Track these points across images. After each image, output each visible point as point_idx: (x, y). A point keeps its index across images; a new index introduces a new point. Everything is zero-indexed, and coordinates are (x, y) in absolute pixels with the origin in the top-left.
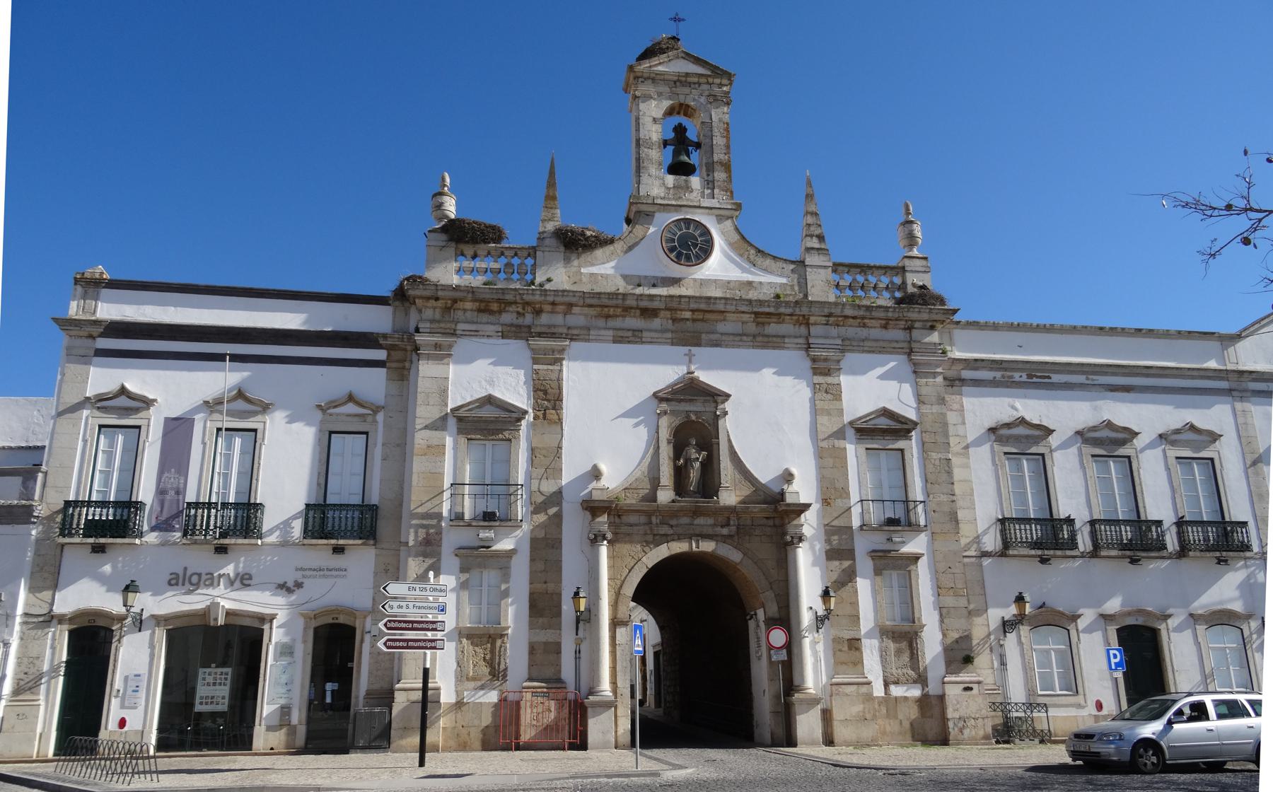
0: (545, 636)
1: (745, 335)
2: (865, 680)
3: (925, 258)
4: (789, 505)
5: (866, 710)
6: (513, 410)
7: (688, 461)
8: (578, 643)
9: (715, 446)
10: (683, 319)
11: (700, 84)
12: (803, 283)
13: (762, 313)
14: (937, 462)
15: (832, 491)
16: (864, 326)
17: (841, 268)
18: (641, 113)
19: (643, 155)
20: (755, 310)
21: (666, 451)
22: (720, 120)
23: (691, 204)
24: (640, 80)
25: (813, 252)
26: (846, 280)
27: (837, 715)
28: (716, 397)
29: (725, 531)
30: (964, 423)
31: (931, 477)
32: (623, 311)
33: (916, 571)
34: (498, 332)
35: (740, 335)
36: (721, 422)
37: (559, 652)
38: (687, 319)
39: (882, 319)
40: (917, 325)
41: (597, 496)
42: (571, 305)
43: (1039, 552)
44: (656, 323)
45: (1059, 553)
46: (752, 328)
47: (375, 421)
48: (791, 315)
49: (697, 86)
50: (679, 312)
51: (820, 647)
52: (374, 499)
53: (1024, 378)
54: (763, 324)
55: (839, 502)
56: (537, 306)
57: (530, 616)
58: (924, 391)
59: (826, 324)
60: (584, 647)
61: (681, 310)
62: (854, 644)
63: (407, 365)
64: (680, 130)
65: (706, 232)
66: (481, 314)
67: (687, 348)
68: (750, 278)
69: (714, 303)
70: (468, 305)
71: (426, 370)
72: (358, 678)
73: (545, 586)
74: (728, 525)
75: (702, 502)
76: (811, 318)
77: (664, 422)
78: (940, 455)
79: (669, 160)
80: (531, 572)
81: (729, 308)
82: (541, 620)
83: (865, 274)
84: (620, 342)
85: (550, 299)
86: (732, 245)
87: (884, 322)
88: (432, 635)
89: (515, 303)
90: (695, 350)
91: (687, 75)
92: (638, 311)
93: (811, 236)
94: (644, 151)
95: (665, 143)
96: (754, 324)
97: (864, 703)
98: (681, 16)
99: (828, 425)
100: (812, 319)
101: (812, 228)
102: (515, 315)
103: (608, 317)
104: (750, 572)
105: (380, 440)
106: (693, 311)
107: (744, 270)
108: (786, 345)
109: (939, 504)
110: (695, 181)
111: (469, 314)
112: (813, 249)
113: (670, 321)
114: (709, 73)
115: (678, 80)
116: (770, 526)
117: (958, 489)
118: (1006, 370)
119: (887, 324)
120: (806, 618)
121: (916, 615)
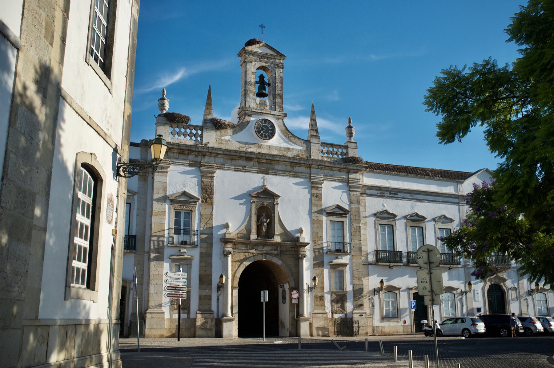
0: (206, 292)
1: (286, 171)
2: (325, 312)
3: (356, 143)
4: (301, 243)
5: (325, 323)
6: (194, 198)
7: (262, 223)
8: (218, 296)
9: (273, 217)
10: (262, 163)
11: (271, 59)
12: (309, 149)
13: (294, 162)
14: (356, 227)
15: (316, 236)
16: (332, 170)
17: (324, 145)
18: (247, 69)
19: (248, 88)
20: (291, 161)
21: (254, 218)
22: (279, 75)
23: (267, 113)
24: (247, 54)
25: (314, 137)
26: (326, 149)
27: (315, 325)
28: (273, 196)
29: (276, 252)
30: (365, 211)
31: (353, 233)
32: (239, 158)
33: (346, 270)
34: (187, 163)
35: (285, 171)
36: (276, 206)
37: (210, 299)
38: (264, 163)
39: (338, 168)
40: (351, 171)
41: (227, 236)
42: (218, 154)
43: (388, 264)
44: (252, 163)
45: (396, 264)
46: (289, 168)
47: (133, 199)
48: (305, 164)
49: (270, 59)
50: (261, 160)
51: (309, 299)
52: (134, 233)
53: (388, 195)
54: (293, 166)
55: (319, 242)
56: (204, 153)
57: (200, 284)
58: (353, 198)
59: (318, 168)
60: (221, 298)
61: (262, 159)
62: (322, 298)
63: (147, 174)
64: (262, 77)
65: (273, 126)
66: (180, 155)
67: (262, 175)
68: (289, 146)
69: (276, 157)
70: (175, 151)
71: (158, 177)
72: (128, 308)
73: (205, 272)
74: (277, 250)
75: (268, 241)
76: (312, 166)
77: (254, 206)
78: (357, 225)
79: (257, 91)
80: (200, 267)
81: (281, 159)
82: (204, 286)
83: (333, 148)
84: (237, 171)
85: (210, 151)
86: (282, 131)
87: (339, 169)
88: (182, 292)
89: (195, 151)
90: (266, 176)
91: (267, 54)
92: (245, 158)
93: (313, 130)
94: (248, 86)
95: (256, 82)
96: (290, 166)
97: (324, 321)
98: (263, 25)
99: (315, 209)
100: (313, 166)
101: (314, 127)
102: (194, 156)
103: (232, 159)
104: (284, 269)
105: (136, 207)
106: (267, 159)
107: (285, 141)
108: (302, 176)
109: (356, 244)
110: (267, 100)
111: (175, 154)
112: (314, 135)
113: (257, 163)
114: (276, 54)
115: (263, 56)
116: (293, 251)
117: (362, 238)
118: (382, 190)
119: (340, 170)
120: (305, 287)
121: (345, 287)
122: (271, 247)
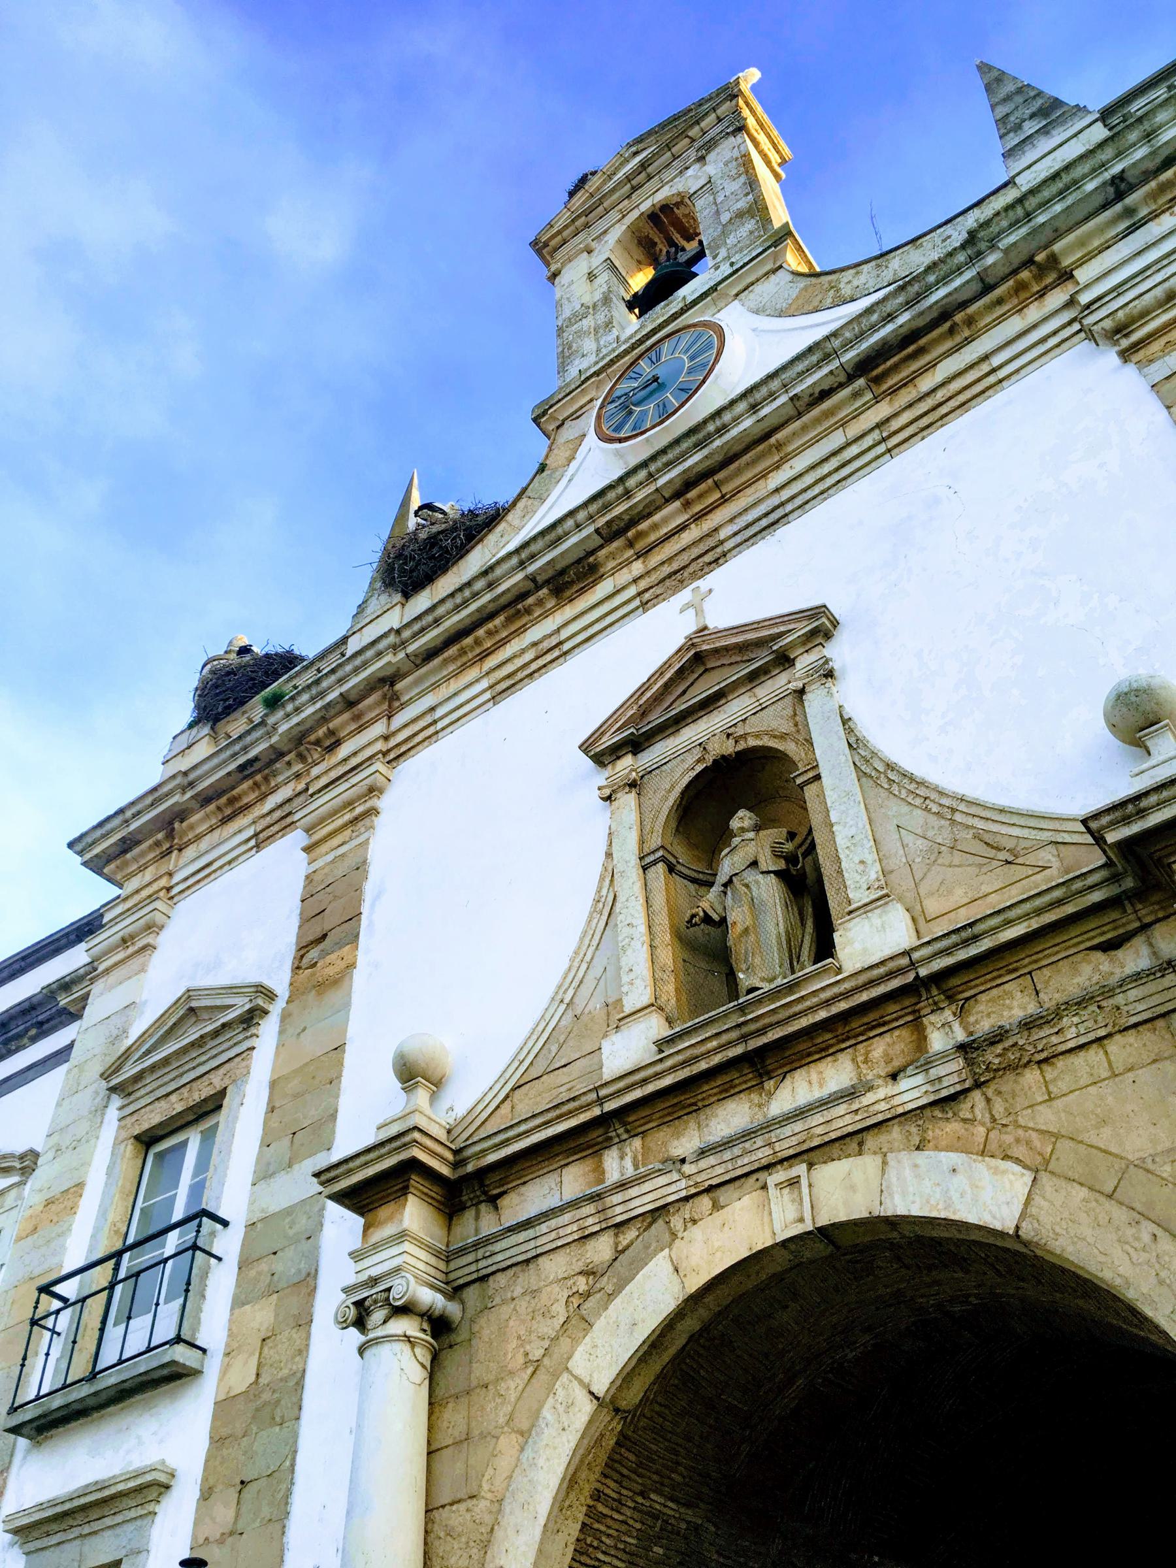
50: (644, 526)
74: (920, 1058)
122: (845, 1060)
